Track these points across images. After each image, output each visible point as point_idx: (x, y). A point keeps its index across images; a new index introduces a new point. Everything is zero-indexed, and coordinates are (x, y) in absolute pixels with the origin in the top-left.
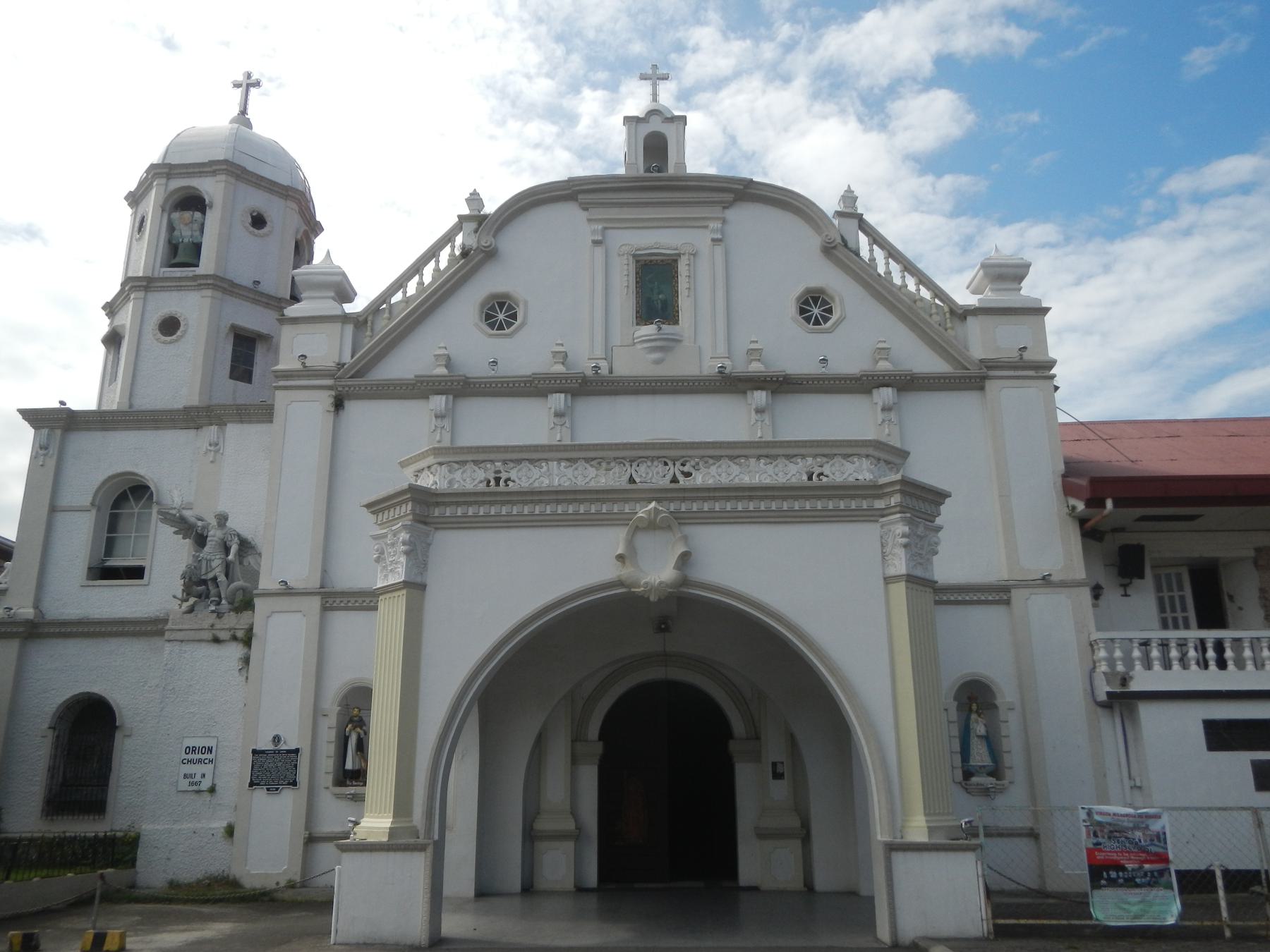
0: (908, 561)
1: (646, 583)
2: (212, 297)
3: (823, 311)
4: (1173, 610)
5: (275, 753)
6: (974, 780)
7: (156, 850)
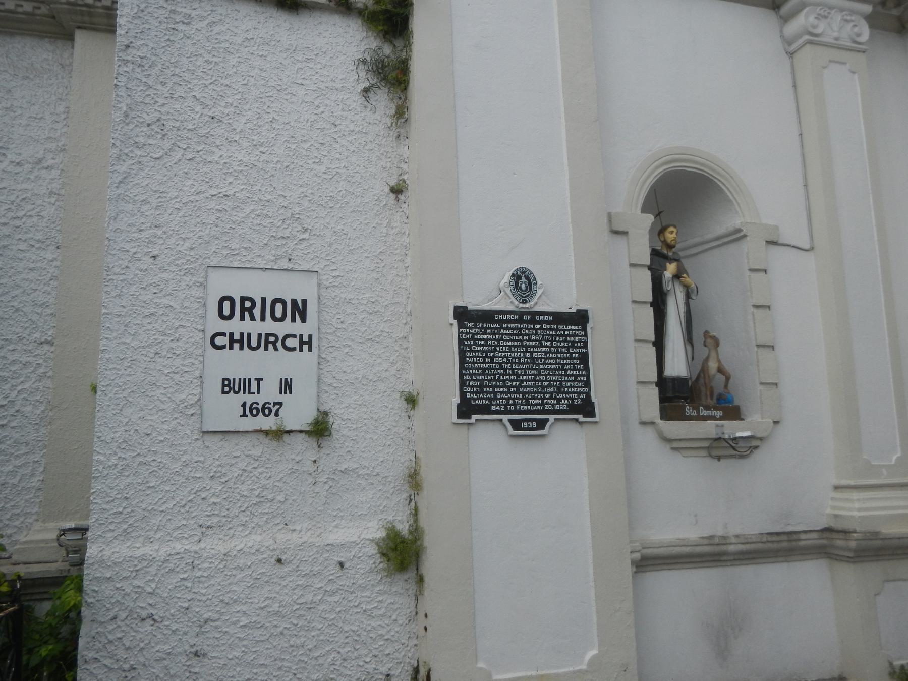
5: (521, 321)
7: (147, 627)
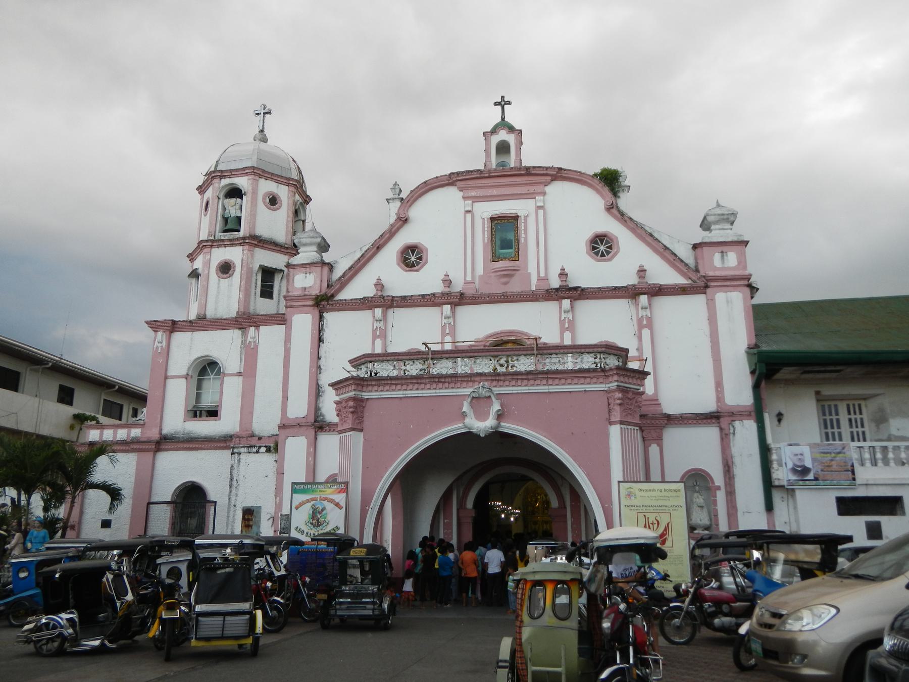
0: (622, 412)
1: (478, 427)
2: (248, 250)
3: (607, 247)
4: (832, 427)
6: (696, 532)
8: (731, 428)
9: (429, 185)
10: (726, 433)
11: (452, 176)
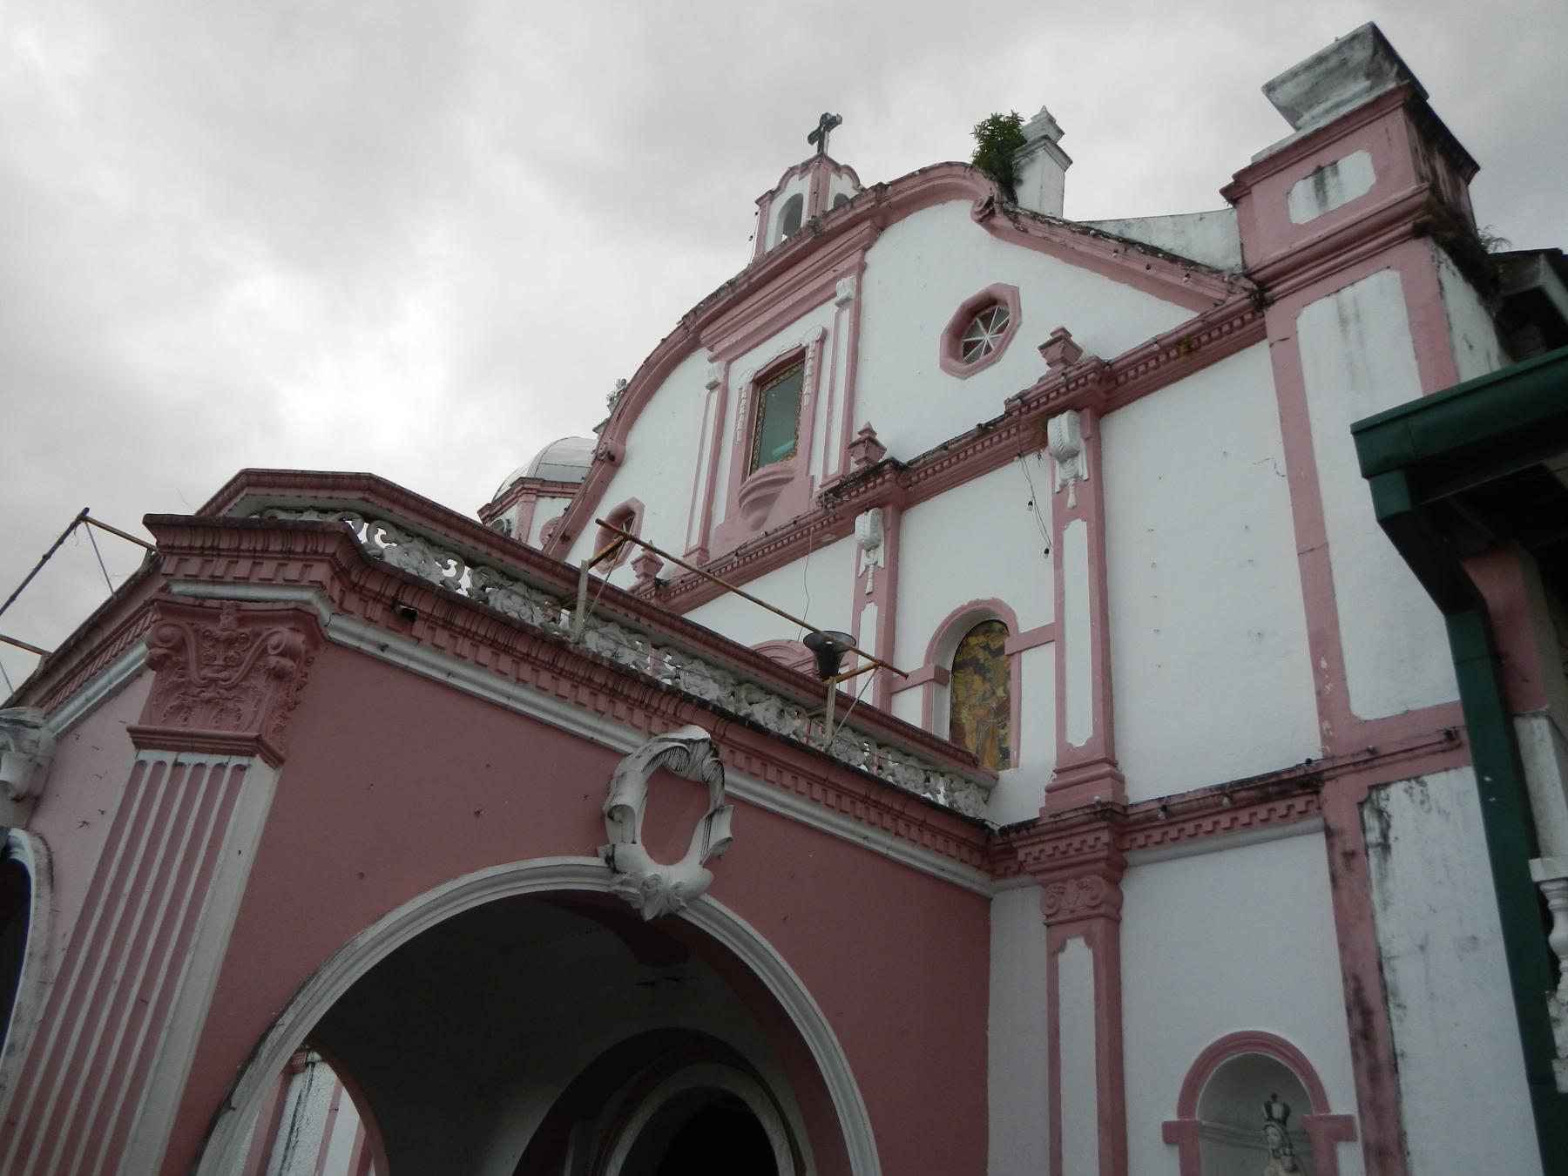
8: (1372, 822)
9: (656, 364)
10: (1350, 847)
11: (688, 323)
